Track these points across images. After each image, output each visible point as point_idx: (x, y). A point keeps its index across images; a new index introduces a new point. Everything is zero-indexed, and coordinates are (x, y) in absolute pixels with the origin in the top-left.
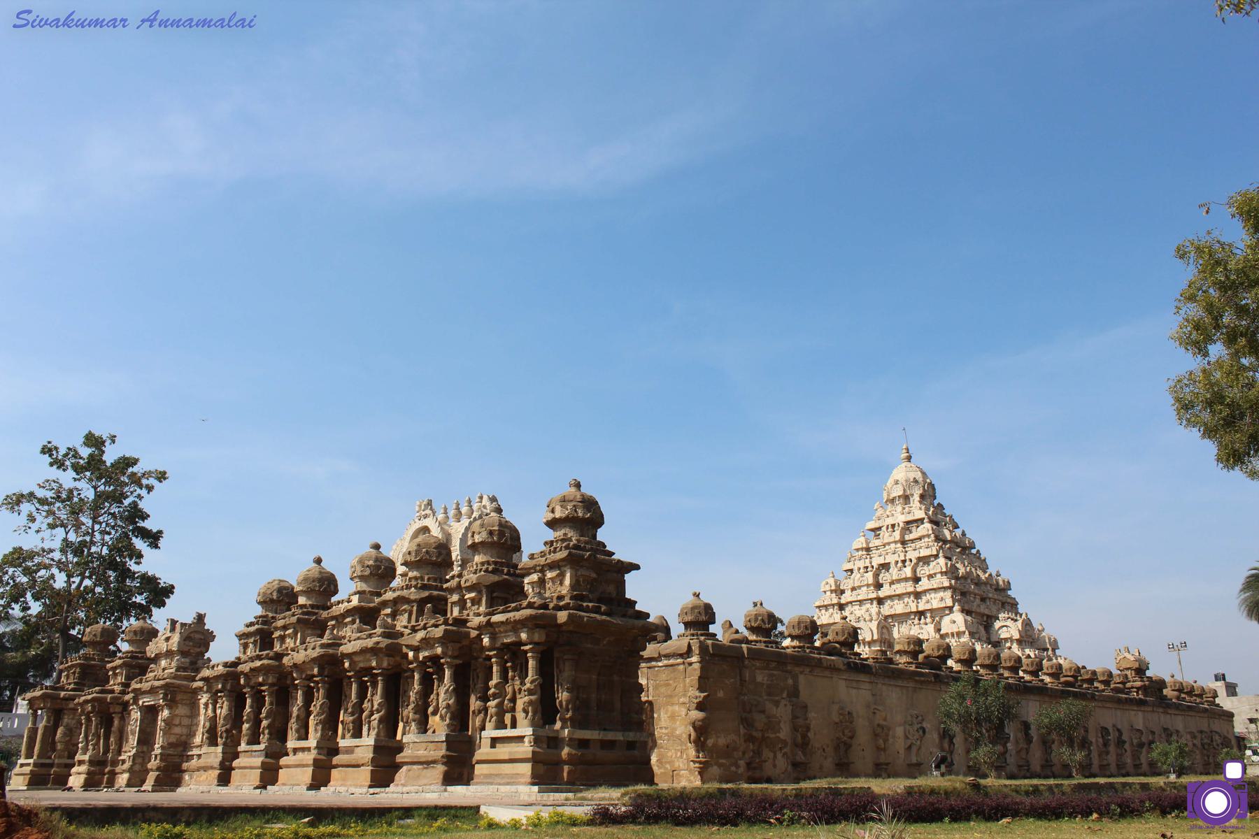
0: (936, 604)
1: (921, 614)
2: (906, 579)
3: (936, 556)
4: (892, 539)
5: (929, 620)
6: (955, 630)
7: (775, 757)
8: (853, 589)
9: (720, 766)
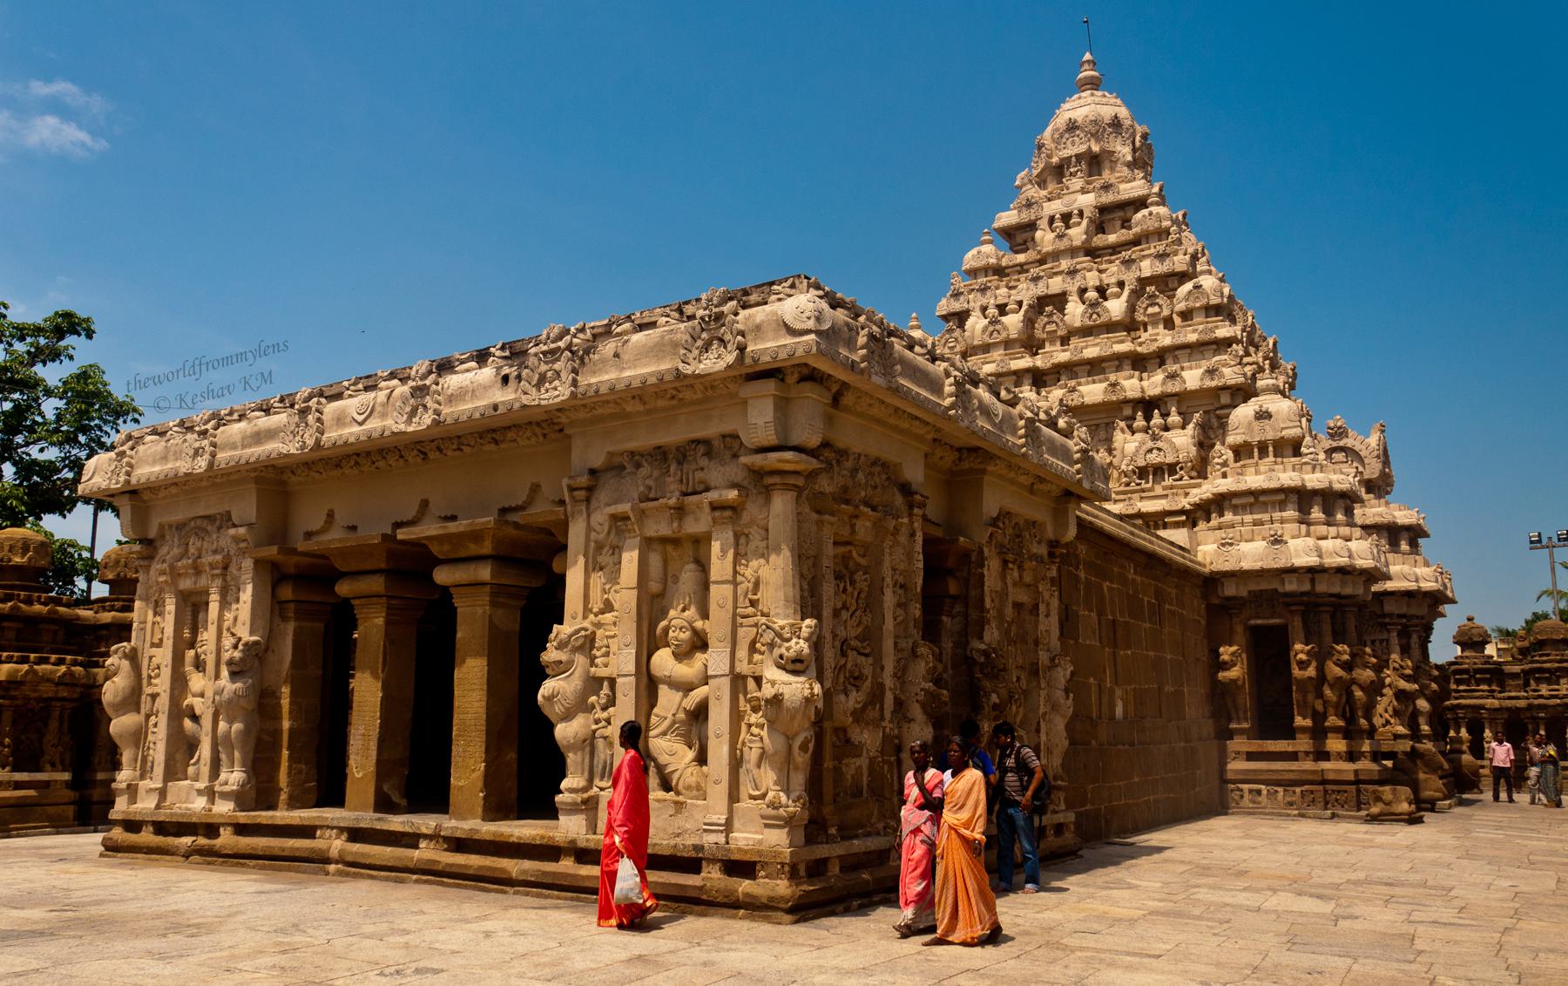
0: (1193, 377)
1: (1148, 405)
2: (1111, 327)
4: (1063, 245)
5: (1174, 418)
6: (1270, 435)
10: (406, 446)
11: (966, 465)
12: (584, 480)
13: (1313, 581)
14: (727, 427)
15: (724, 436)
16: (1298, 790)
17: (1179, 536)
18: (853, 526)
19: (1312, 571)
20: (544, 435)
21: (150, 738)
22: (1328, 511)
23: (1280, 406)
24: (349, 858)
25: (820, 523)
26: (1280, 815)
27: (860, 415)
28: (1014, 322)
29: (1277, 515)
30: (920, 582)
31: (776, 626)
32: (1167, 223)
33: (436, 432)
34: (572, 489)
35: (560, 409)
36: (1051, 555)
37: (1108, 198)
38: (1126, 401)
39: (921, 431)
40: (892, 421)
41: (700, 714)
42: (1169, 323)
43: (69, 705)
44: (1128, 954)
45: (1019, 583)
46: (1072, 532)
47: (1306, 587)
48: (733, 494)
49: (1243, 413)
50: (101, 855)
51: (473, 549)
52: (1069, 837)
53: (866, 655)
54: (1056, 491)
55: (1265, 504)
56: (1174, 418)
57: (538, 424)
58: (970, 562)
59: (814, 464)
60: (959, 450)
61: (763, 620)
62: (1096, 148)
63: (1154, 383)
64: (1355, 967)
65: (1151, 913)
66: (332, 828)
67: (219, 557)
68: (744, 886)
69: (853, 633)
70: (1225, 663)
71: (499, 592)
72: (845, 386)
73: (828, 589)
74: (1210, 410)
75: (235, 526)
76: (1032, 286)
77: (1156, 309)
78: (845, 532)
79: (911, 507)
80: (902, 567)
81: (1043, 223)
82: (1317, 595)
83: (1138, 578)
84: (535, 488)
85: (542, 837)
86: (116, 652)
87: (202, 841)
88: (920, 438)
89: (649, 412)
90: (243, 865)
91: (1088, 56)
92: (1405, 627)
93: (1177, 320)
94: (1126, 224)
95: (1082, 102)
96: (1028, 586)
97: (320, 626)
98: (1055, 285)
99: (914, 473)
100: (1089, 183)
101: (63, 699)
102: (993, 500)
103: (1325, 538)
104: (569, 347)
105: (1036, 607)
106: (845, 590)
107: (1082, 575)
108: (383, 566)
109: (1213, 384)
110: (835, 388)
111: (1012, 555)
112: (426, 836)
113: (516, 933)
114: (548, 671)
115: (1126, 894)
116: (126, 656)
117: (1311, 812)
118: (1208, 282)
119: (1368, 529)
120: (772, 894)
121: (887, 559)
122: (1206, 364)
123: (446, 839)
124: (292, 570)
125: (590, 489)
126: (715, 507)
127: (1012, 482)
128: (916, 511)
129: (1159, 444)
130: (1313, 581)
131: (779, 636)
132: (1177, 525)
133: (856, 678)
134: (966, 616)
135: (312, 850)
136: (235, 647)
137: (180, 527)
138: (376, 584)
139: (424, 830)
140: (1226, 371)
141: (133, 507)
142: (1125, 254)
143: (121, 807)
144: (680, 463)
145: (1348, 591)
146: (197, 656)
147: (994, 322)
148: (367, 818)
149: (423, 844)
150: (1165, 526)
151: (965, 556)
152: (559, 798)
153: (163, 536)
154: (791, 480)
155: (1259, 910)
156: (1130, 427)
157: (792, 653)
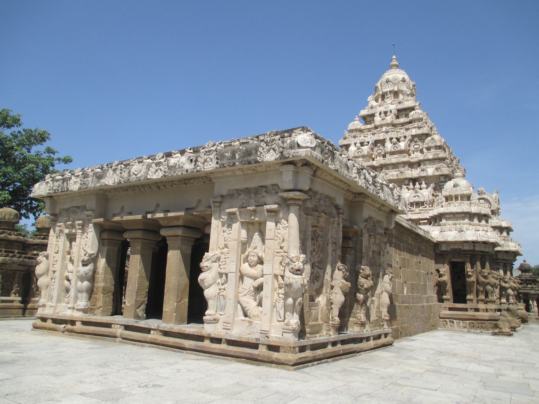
0: (430, 171)
1: (414, 181)
4: (384, 122)
5: (424, 185)
10: (152, 184)
11: (357, 199)
12: (219, 199)
13: (474, 246)
14: (274, 182)
15: (272, 185)
16: (468, 322)
17: (426, 228)
18: (318, 220)
19: (473, 242)
20: (204, 182)
21: (52, 287)
22: (480, 221)
23: (463, 182)
24: (124, 337)
25: (307, 219)
26: (461, 331)
27: (323, 179)
29: (462, 222)
30: (341, 242)
31: (290, 257)
32: (421, 116)
33: (164, 179)
34: (214, 202)
35: (211, 173)
36: (385, 233)
37: (400, 107)
38: (406, 179)
39: (342, 185)
40: (334, 182)
41: (259, 289)
42: (422, 151)
43: (22, 273)
44: (424, 389)
45: (374, 243)
46: (393, 225)
47: (472, 248)
48: (275, 206)
49: (449, 185)
50: (32, 330)
51: (175, 223)
52: (389, 339)
53: (321, 269)
54: (388, 210)
55: (457, 217)
57: (202, 178)
58: (358, 235)
59: (305, 196)
60: (355, 193)
61: (285, 254)
62: (396, 89)
64: (513, 398)
65: (427, 371)
66: (118, 324)
67: (81, 222)
68: (275, 355)
69: (316, 260)
70: (442, 275)
71: (184, 238)
72: (318, 168)
73: (309, 243)
74: (438, 182)
75: (87, 210)
76: (373, 136)
77: (417, 146)
78: (315, 223)
79: (339, 214)
80: (335, 236)
81: (377, 114)
82: (475, 251)
83: (412, 243)
84: (199, 201)
85: (198, 332)
86: (41, 255)
87: (69, 326)
88: (342, 189)
89: (244, 175)
90: (84, 337)
91: (394, 57)
92: (505, 264)
93: (425, 150)
94: (407, 116)
95: (391, 73)
96: (377, 245)
97: (116, 249)
98: (381, 136)
99: (340, 201)
100: (394, 101)
101: (21, 271)
102: (367, 212)
103: (479, 231)
104: (216, 150)
105: (380, 252)
106: (314, 244)
107: (394, 241)
108: (141, 228)
109: (438, 174)
110: (314, 169)
111: (372, 233)
112: (153, 329)
113: (189, 370)
114: (203, 270)
115: (414, 362)
116: (45, 256)
117: (472, 330)
118: (436, 137)
119: (494, 228)
120: (286, 359)
121: (330, 232)
122: (435, 166)
123: (161, 331)
124: (107, 228)
125: (221, 202)
126: (269, 211)
127: (373, 206)
128: (340, 215)
129: (418, 194)
130: (474, 246)
131: (291, 261)
132: (424, 224)
133: (317, 277)
134: (356, 255)
135: (111, 332)
136: (85, 255)
137: (67, 210)
138: (139, 234)
139: (153, 327)
140: (443, 169)
141: (50, 202)
142: (407, 126)
143: (40, 312)
144: (255, 194)
145: (486, 250)
146: (71, 258)
148: (132, 322)
149: (152, 332)
150: (420, 224)
151: (356, 233)
152: (204, 318)
153: (61, 213)
154: (298, 202)
155: (466, 371)
156: (407, 188)
157: (297, 268)
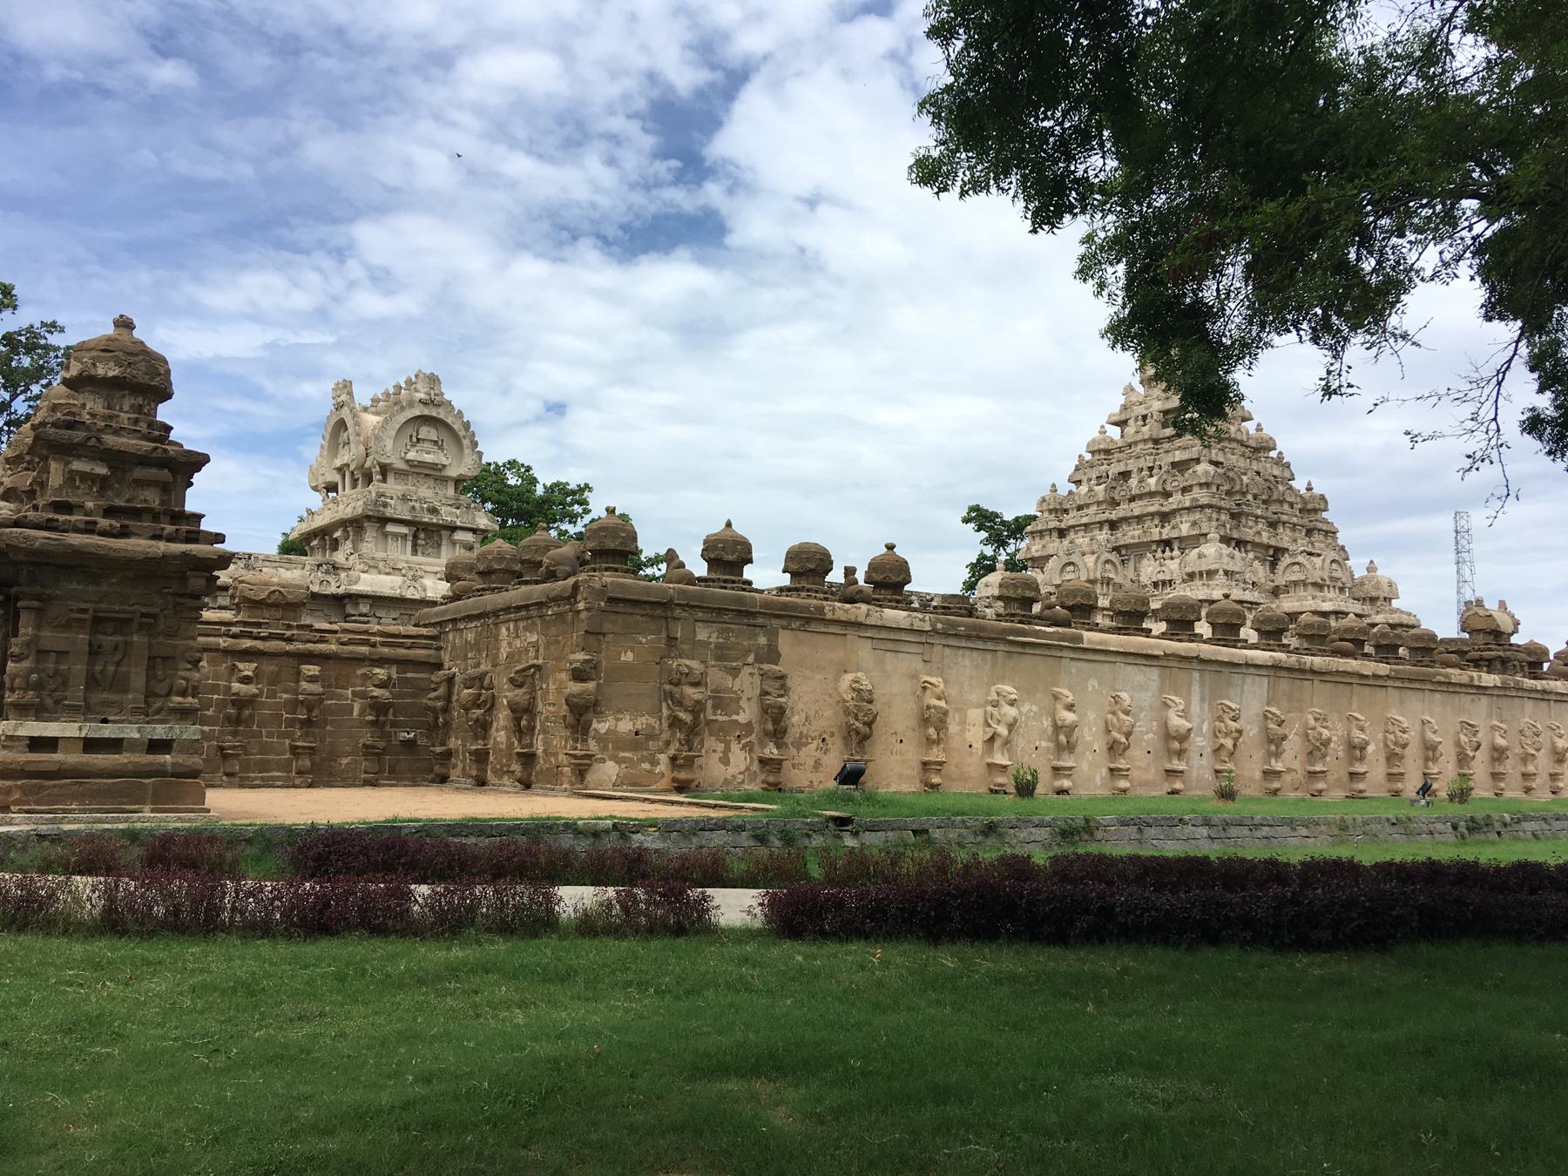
0: (1185, 530)
1: (1167, 543)
3: (1198, 461)
4: (1140, 437)
5: (1176, 552)
7: (727, 750)
8: (1080, 508)
9: (619, 761)
28: (1100, 490)
56: (1176, 552)
63: (1167, 533)
98: (1132, 465)
147: (1090, 490)
